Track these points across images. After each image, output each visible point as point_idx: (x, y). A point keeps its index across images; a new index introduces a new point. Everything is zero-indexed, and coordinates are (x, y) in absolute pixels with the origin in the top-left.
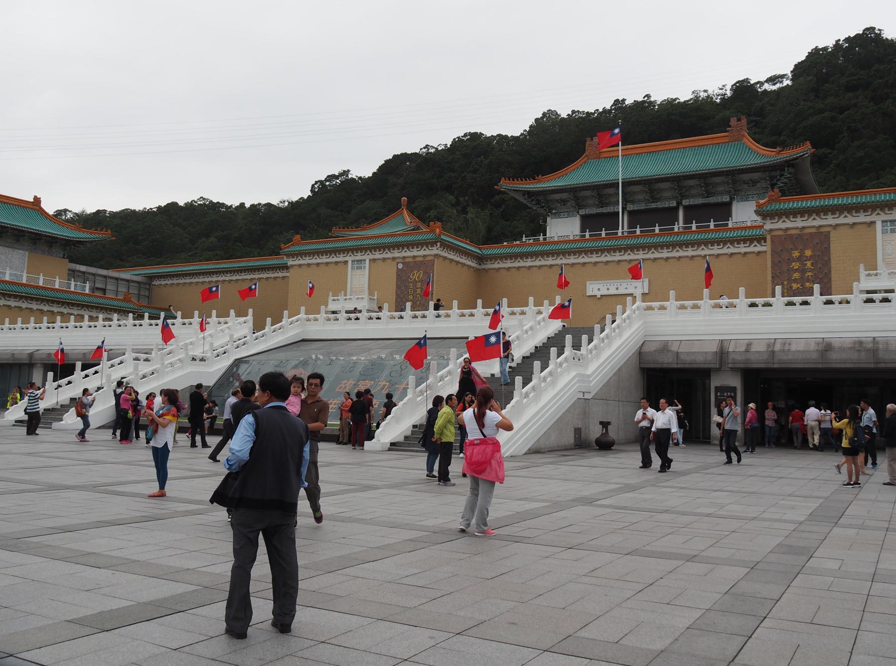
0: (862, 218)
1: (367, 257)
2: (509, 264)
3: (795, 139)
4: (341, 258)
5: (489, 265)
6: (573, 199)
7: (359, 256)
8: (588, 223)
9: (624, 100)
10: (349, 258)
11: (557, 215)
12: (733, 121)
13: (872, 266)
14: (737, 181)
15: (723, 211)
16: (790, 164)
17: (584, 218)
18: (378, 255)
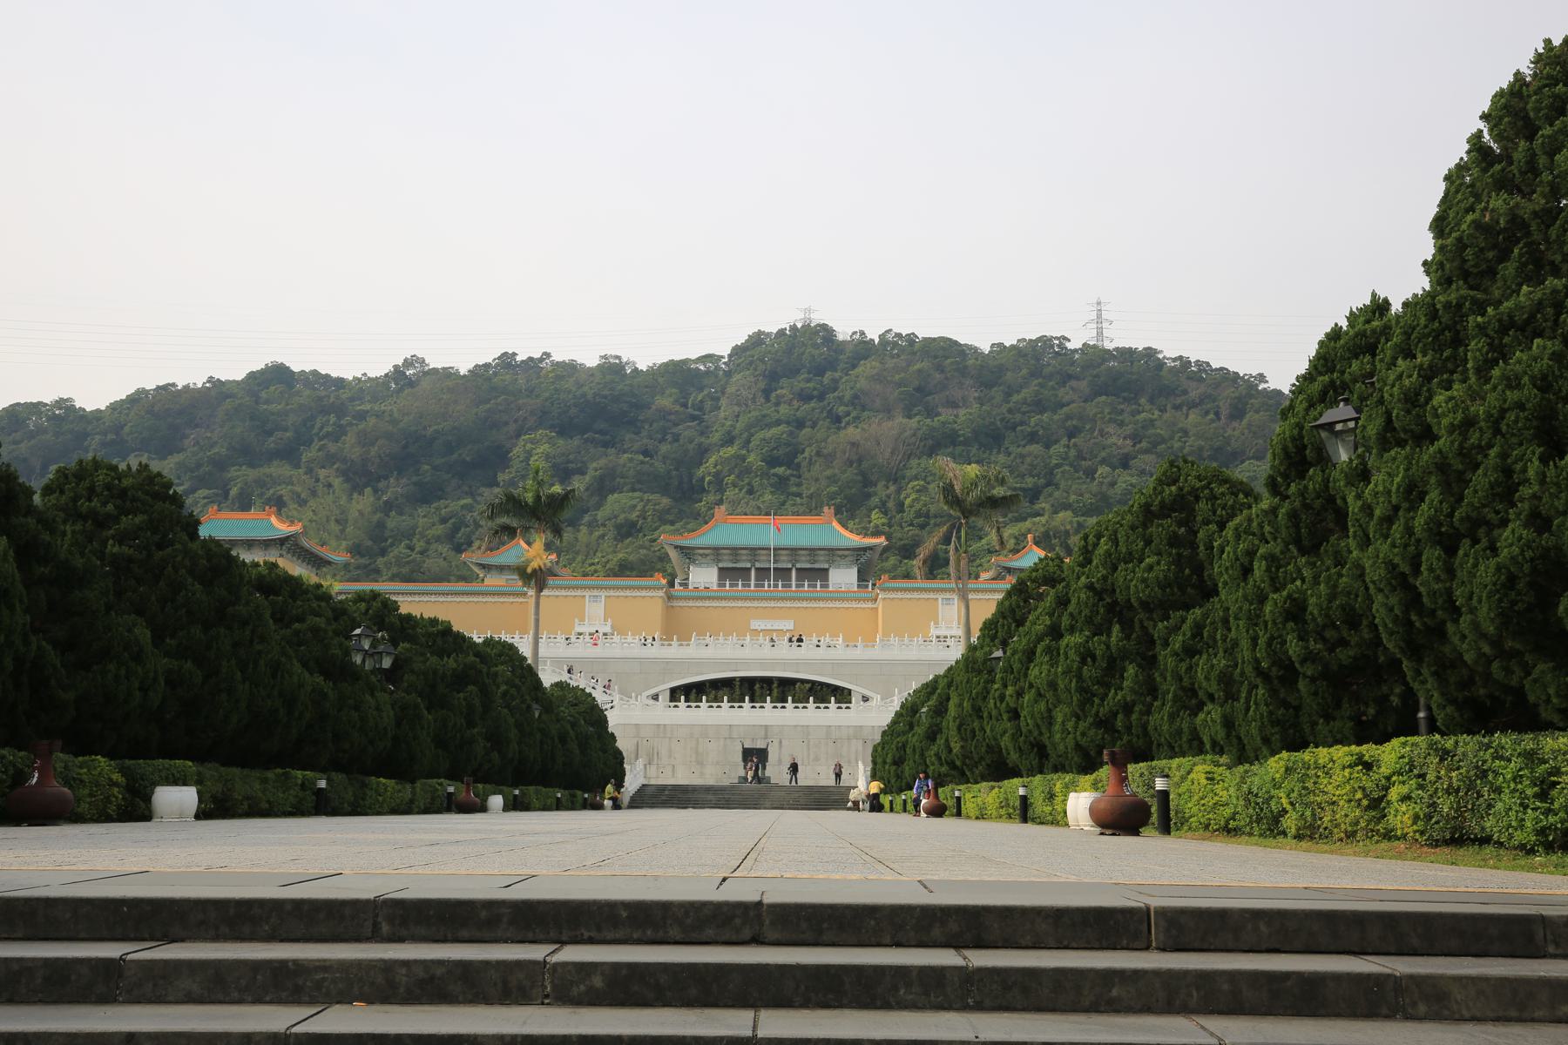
0: (932, 596)
1: (603, 594)
2: (691, 603)
3: (876, 534)
4: (579, 593)
5: (675, 604)
6: (716, 552)
7: (595, 593)
8: (724, 573)
9: (515, 354)
10: (587, 593)
11: (700, 565)
12: (826, 509)
13: (936, 623)
14: (835, 554)
15: (823, 574)
16: (871, 548)
17: (720, 569)
18: (612, 593)
